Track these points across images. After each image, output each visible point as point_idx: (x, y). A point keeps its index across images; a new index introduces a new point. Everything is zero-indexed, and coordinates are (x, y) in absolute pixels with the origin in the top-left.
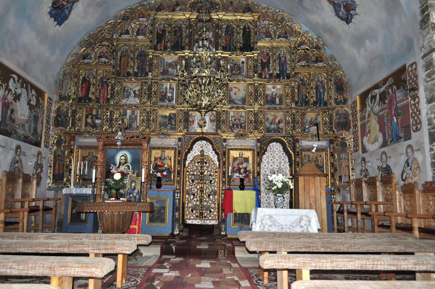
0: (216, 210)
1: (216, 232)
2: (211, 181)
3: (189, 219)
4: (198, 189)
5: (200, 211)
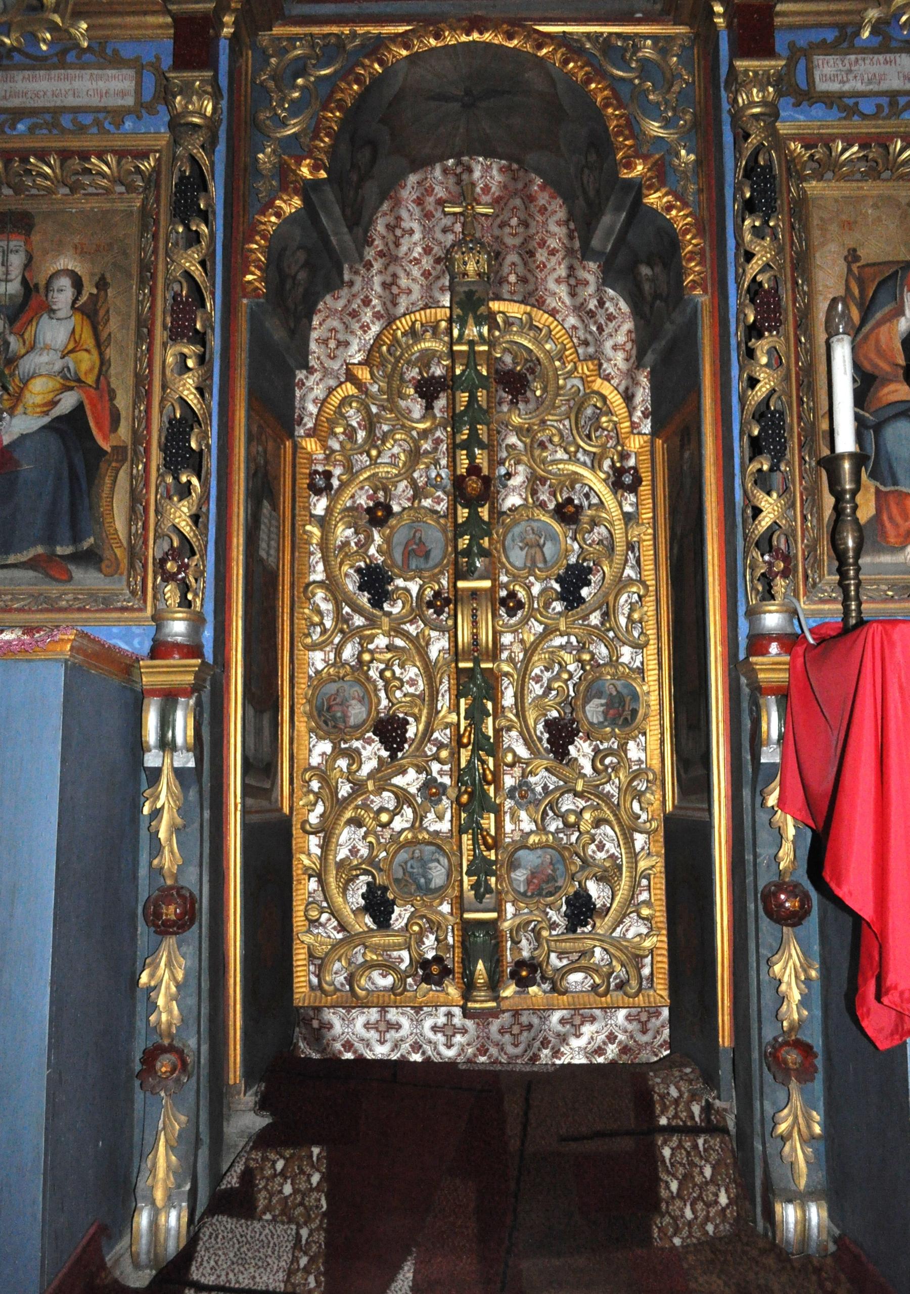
0: (654, 896)
1: (692, 1203)
2: (573, 581)
3: (354, 1001)
4: (429, 671)
5: (460, 905)
